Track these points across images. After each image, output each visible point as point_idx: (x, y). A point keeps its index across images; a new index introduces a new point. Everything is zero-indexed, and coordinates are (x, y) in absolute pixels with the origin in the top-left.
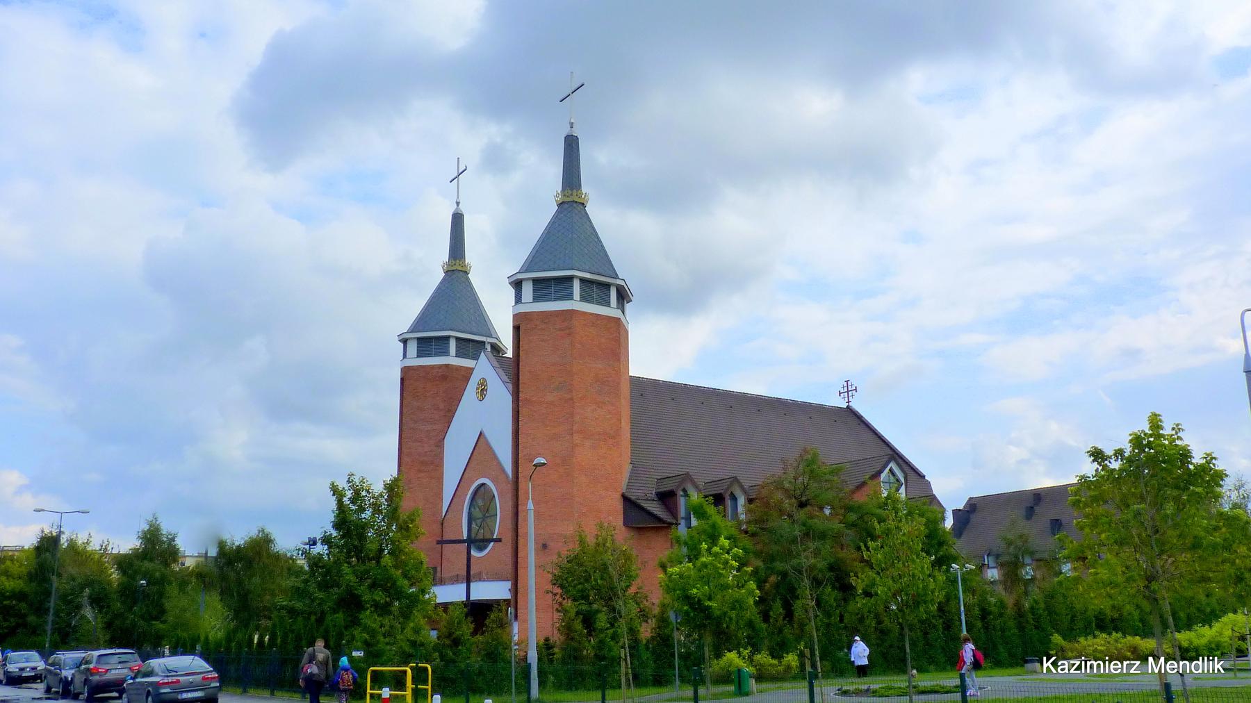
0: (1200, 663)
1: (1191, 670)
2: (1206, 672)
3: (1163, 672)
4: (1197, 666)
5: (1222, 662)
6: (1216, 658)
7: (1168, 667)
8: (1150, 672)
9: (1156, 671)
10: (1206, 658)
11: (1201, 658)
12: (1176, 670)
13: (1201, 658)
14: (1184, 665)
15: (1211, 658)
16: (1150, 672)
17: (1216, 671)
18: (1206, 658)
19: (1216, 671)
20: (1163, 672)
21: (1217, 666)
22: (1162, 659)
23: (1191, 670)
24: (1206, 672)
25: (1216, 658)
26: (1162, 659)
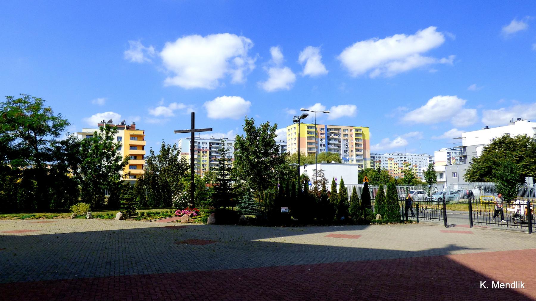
0: (514, 284)
1: (510, 287)
3: (498, 288)
5: (524, 284)
6: (521, 282)
8: (493, 288)
9: (496, 287)
11: (515, 282)
12: (504, 287)
13: (515, 282)
14: (508, 285)
15: (519, 282)
16: (493, 288)
20: (498, 288)
21: (522, 285)
23: (510, 287)
25: (521, 282)
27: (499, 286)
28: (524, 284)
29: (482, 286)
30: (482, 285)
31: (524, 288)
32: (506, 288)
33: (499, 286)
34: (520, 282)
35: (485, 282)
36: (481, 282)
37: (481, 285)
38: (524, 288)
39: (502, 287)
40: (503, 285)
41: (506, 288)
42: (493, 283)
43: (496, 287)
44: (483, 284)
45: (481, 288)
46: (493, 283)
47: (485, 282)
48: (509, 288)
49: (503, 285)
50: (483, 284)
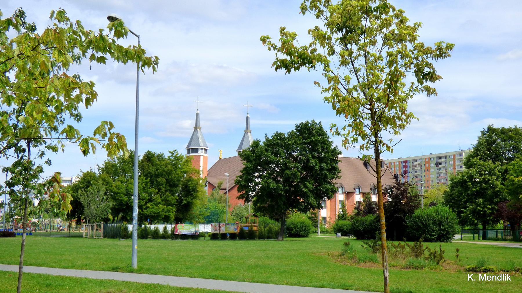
2: (503, 280)
3: (485, 280)
4: (499, 278)
5: (510, 276)
7: (487, 278)
8: (480, 280)
9: (483, 280)
10: (503, 274)
11: (501, 274)
12: (491, 280)
13: (501, 274)
15: (505, 274)
16: (480, 280)
17: (507, 280)
18: (503, 274)
19: (507, 280)
20: (485, 280)
21: (508, 278)
22: (485, 275)
24: (503, 280)
25: (507, 274)
26: (485, 275)
27: (486, 278)
28: (510, 276)
29: (470, 278)
30: (470, 278)
31: (510, 280)
32: (493, 280)
33: (486, 278)
34: (506, 275)
35: (472, 274)
36: (469, 274)
37: (469, 278)
38: (510, 280)
39: (489, 279)
40: (489, 277)
41: (493, 280)
42: (480, 275)
43: (483, 280)
44: (470, 277)
45: (469, 280)
46: (480, 275)
47: (472, 274)
48: (496, 280)
49: (490, 277)
50: (470, 277)
